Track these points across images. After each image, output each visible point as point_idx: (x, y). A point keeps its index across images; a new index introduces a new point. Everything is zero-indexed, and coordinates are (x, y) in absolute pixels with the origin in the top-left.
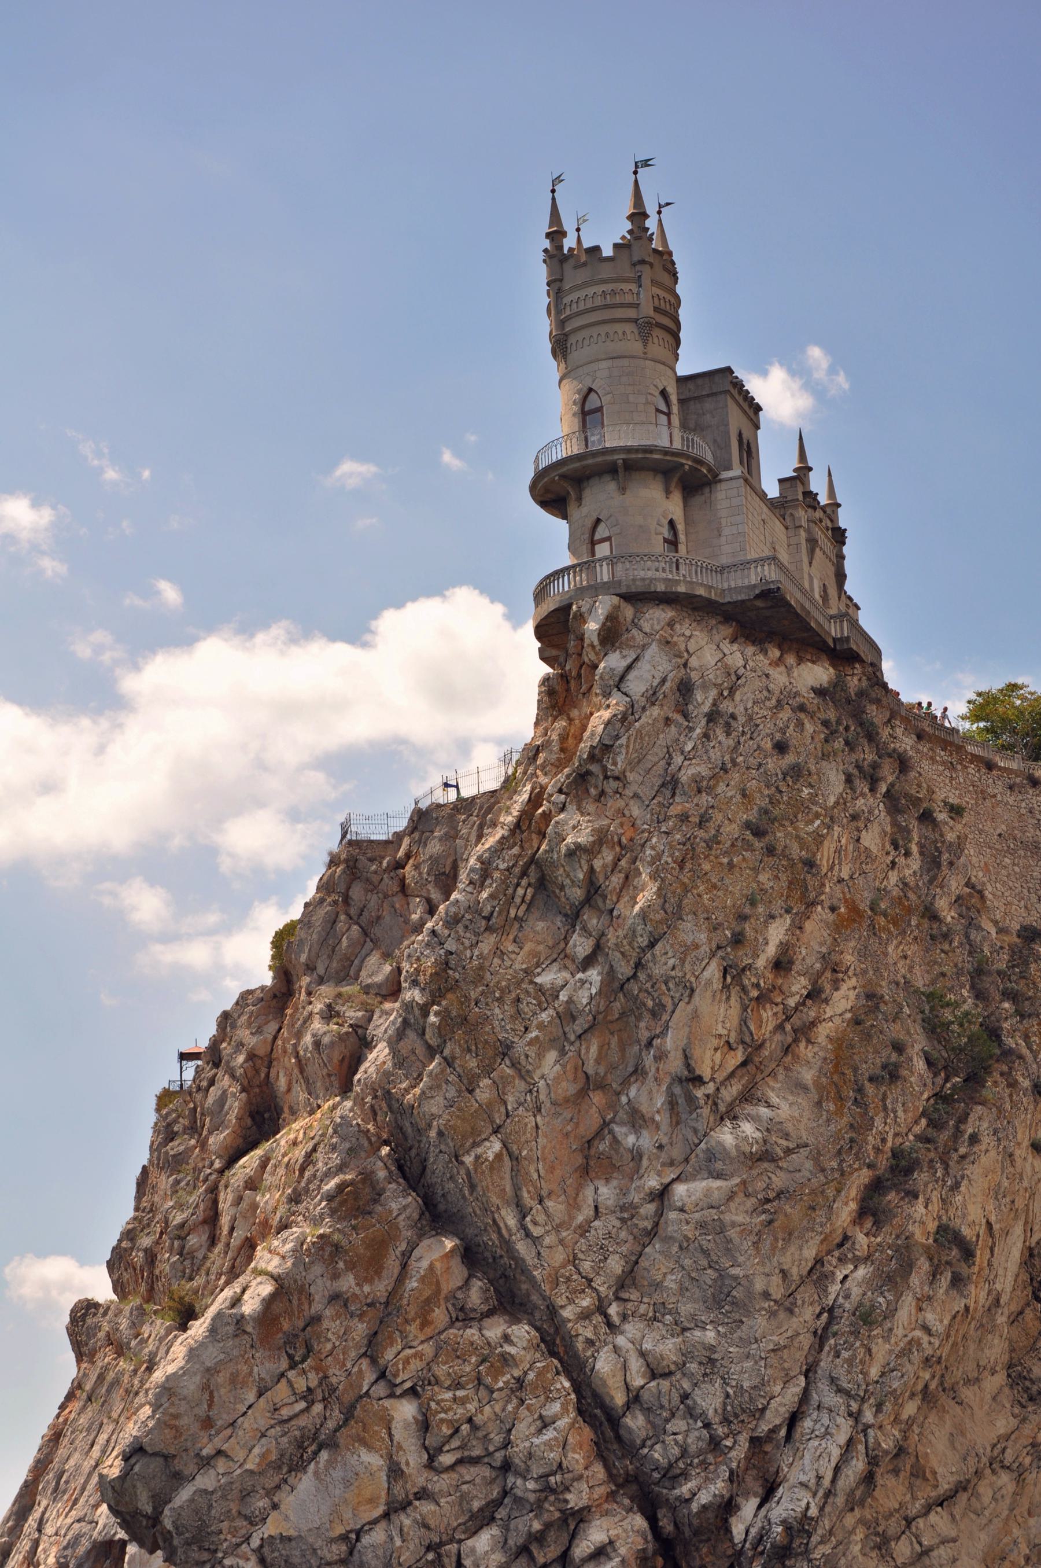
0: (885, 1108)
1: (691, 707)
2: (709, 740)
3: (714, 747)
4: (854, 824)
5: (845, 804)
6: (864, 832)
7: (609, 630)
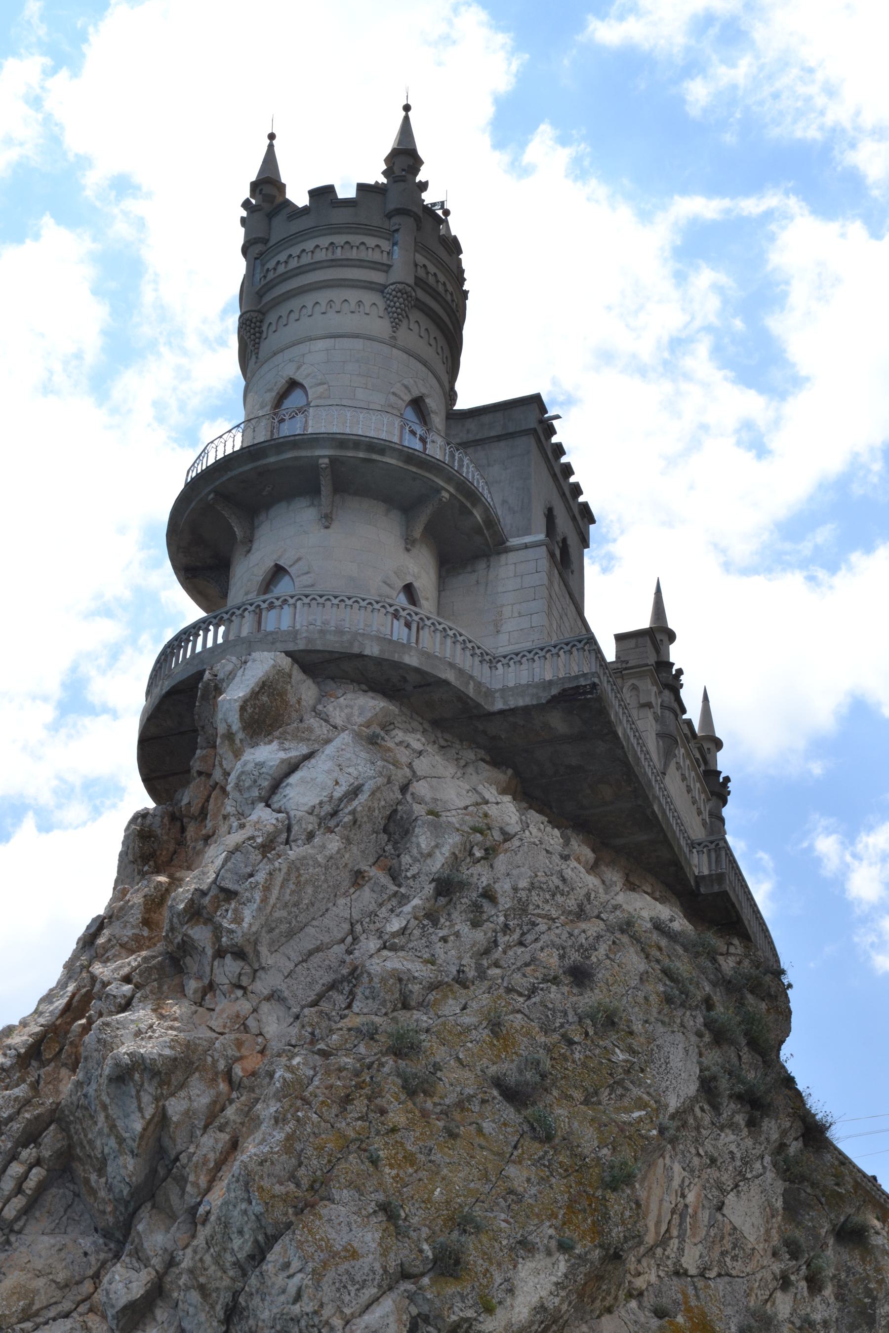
1: (406, 859)
2: (435, 923)
3: (444, 939)
4: (713, 1173)
5: (698, 1128)
6: (731, 1196)
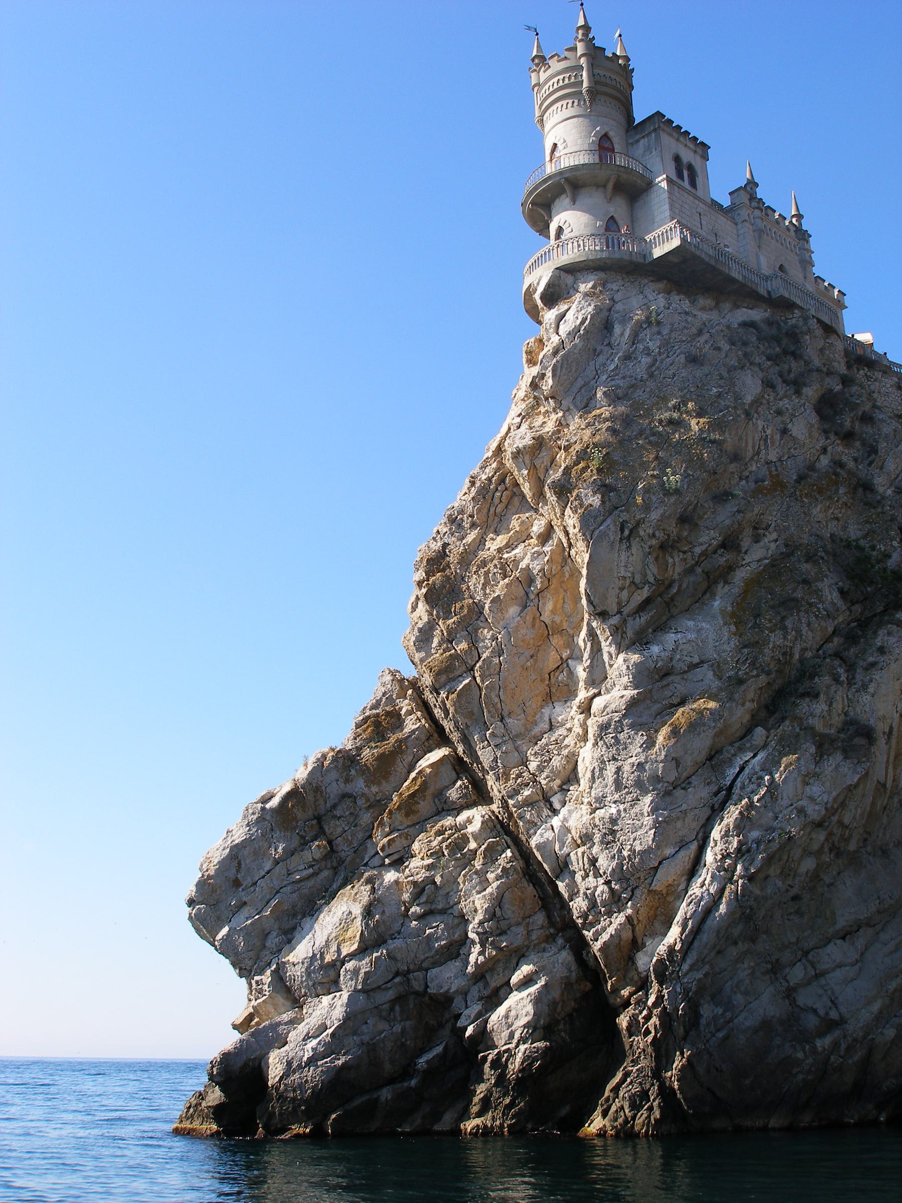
0: (784, 628)
4: (779, 418)
5: (768, 403)
7: (552, 294)
